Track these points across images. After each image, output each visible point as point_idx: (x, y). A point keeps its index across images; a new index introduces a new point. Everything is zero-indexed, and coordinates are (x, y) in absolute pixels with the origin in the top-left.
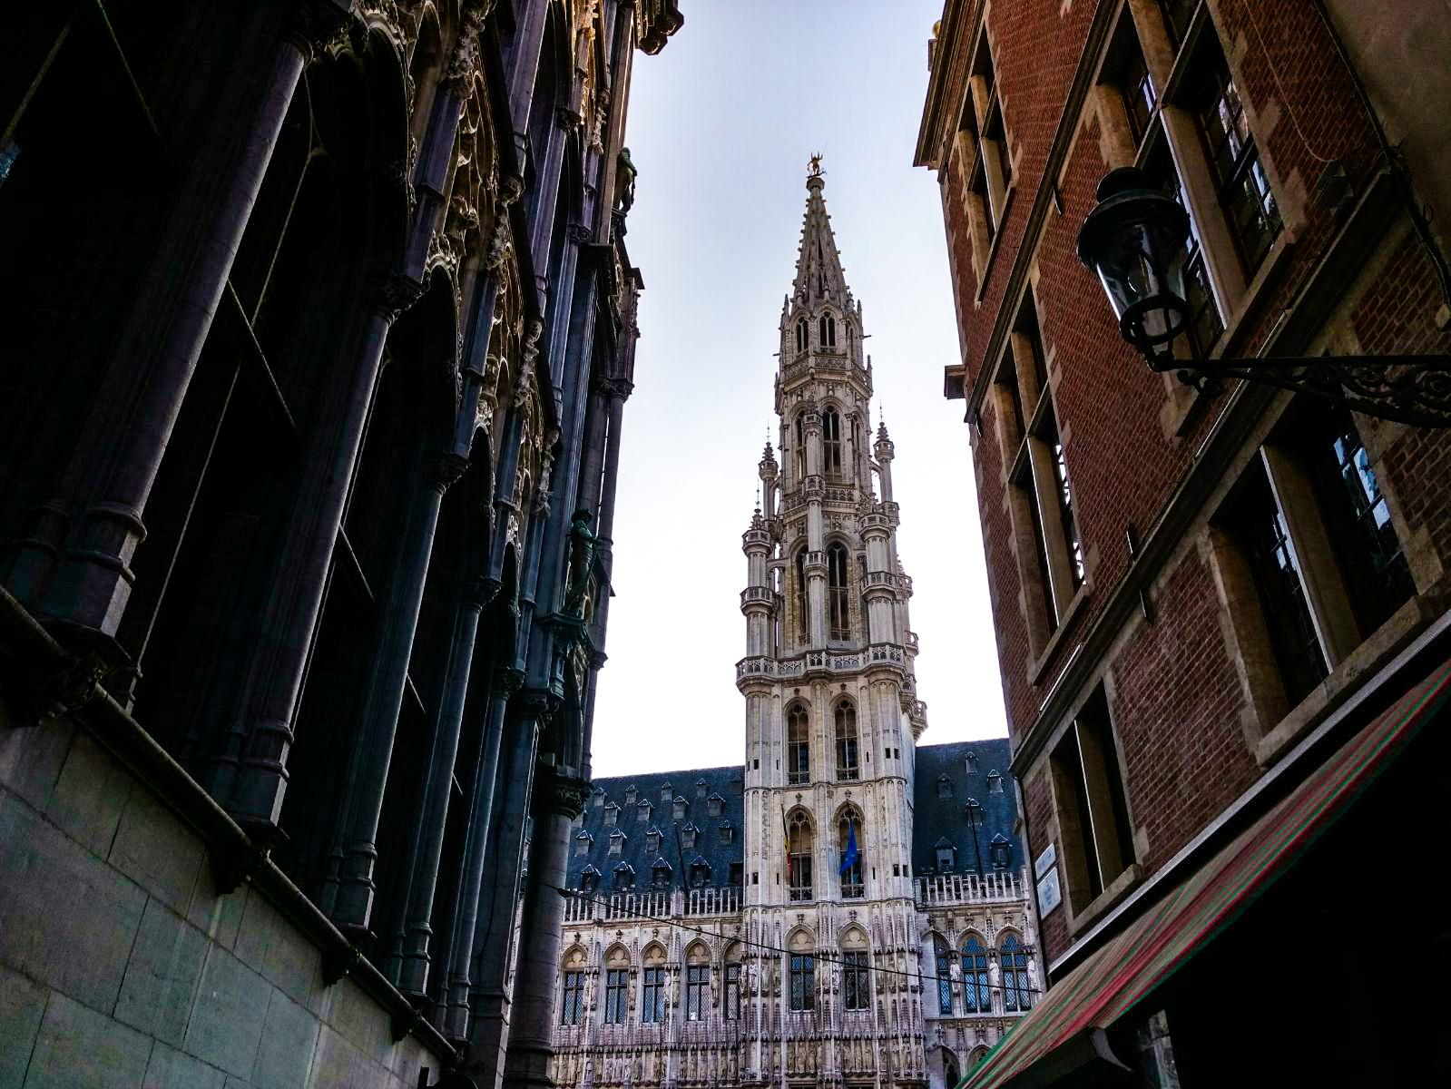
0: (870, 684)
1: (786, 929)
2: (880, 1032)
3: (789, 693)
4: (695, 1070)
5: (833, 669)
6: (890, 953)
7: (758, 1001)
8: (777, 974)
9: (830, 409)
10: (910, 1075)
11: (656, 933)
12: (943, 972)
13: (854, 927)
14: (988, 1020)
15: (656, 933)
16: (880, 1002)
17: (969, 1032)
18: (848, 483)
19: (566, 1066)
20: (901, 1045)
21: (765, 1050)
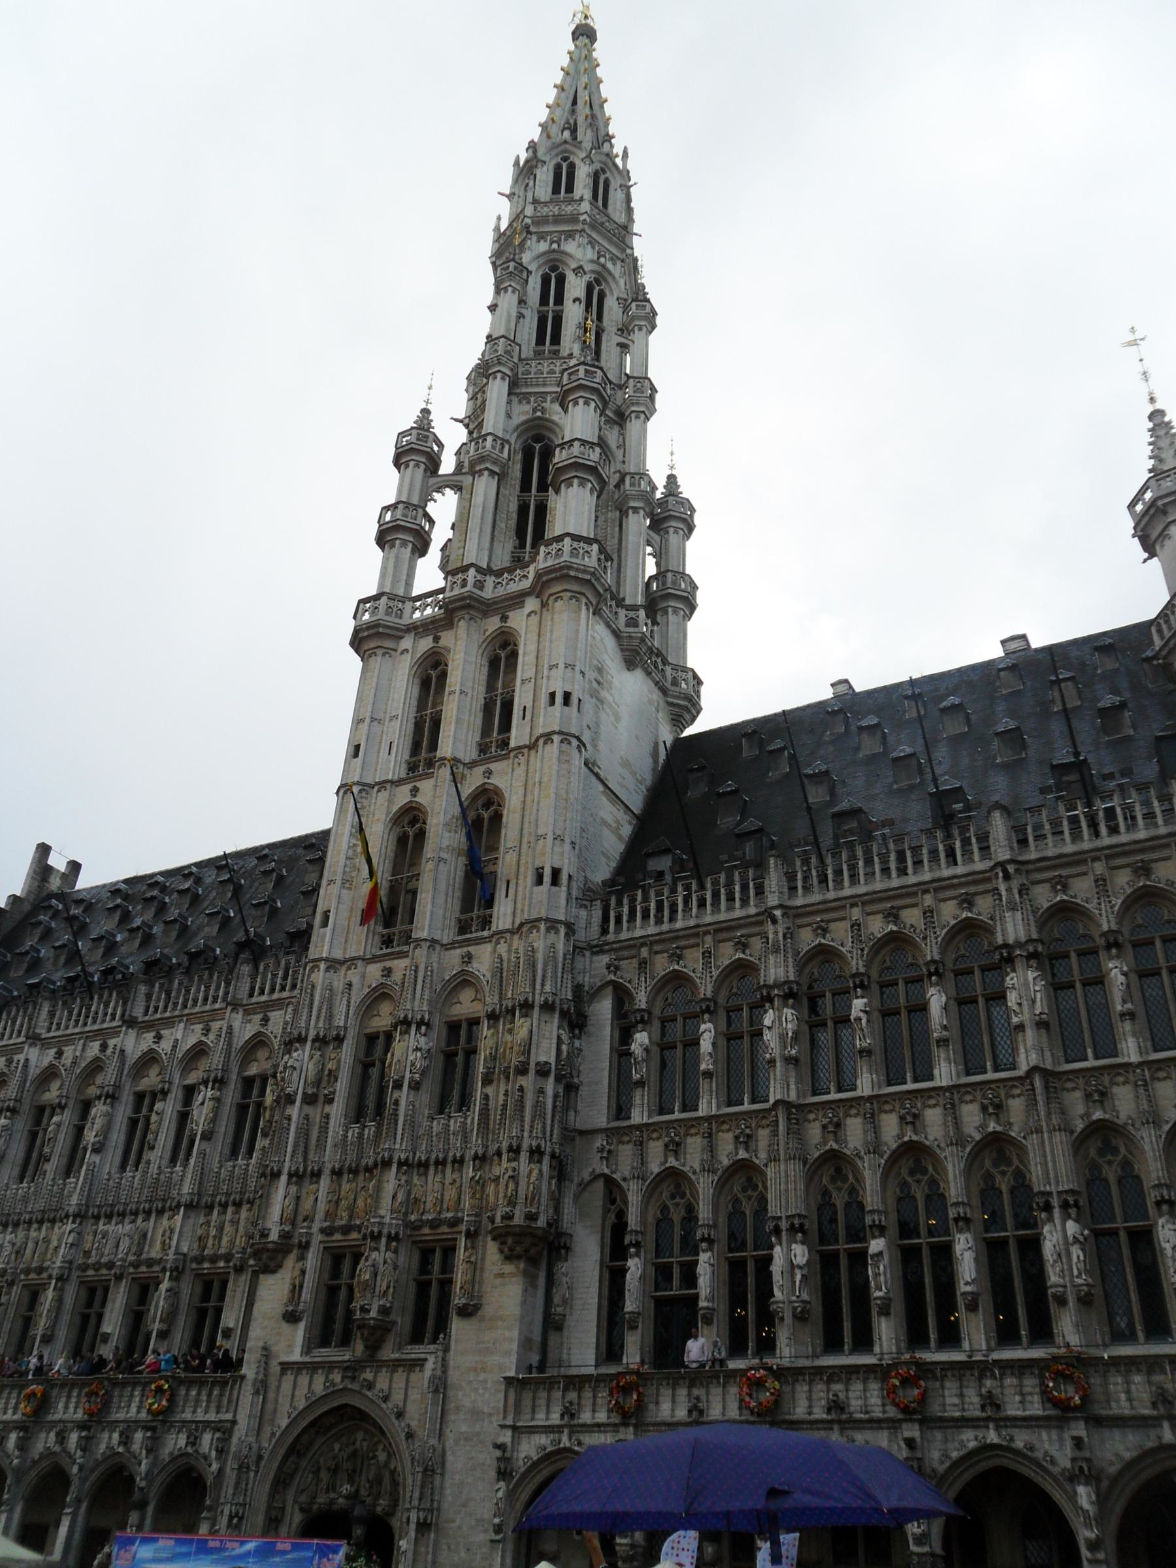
0: (544, 605)
1: (357, 996)
2: (476, 1145)
3: (426, 644)
4: (218, 1237)
5: (488, 593)
6: (511, 1012)
7: (294, 1111)
8: (330, 1066)
9: (554, 268)
10: (508, 1217)
11: (207, 1031)
12: (621, 1052)
13: (464, 980)
14: (689, 1124)
15: (207, 1031)
16: (486, 1097)
17: (655, 1148)
18: (566, 354)
19: (47, 1240)
20: (505, 1164)
21: (293, 1189)
